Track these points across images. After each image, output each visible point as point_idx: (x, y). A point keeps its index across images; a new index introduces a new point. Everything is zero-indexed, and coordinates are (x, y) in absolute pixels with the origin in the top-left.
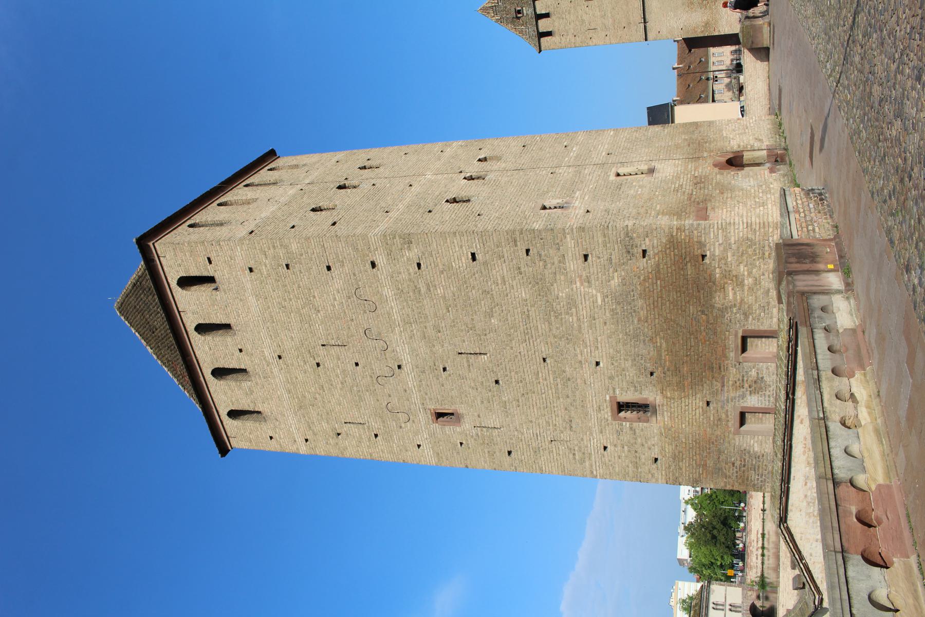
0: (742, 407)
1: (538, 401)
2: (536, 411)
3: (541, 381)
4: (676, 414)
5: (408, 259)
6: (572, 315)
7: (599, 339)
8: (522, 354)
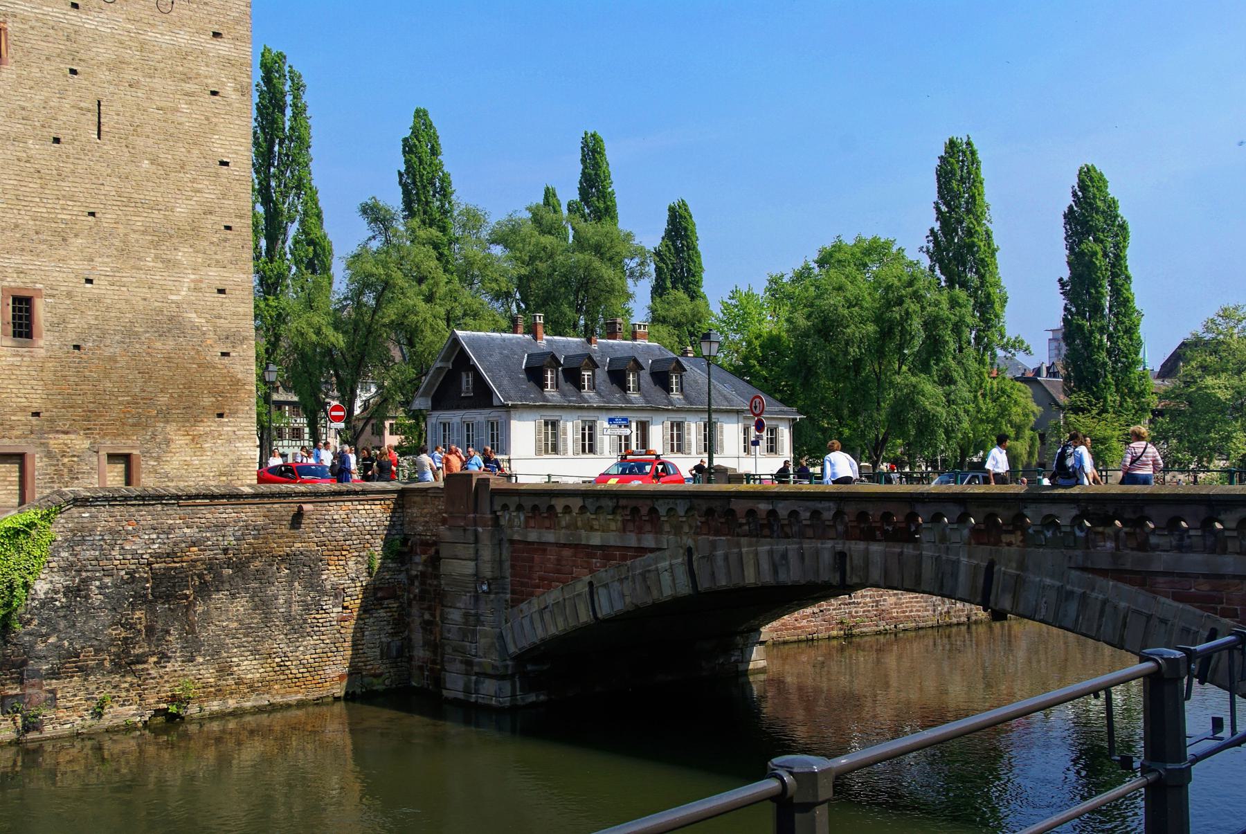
0: (33, 456)
1: (28, 189)
2: (11, 182)
3: (61, 202)
4: (18, 372)
5: (224, 84)
6: (153, 261)
7: (124, 289)
8: (102, 187)
